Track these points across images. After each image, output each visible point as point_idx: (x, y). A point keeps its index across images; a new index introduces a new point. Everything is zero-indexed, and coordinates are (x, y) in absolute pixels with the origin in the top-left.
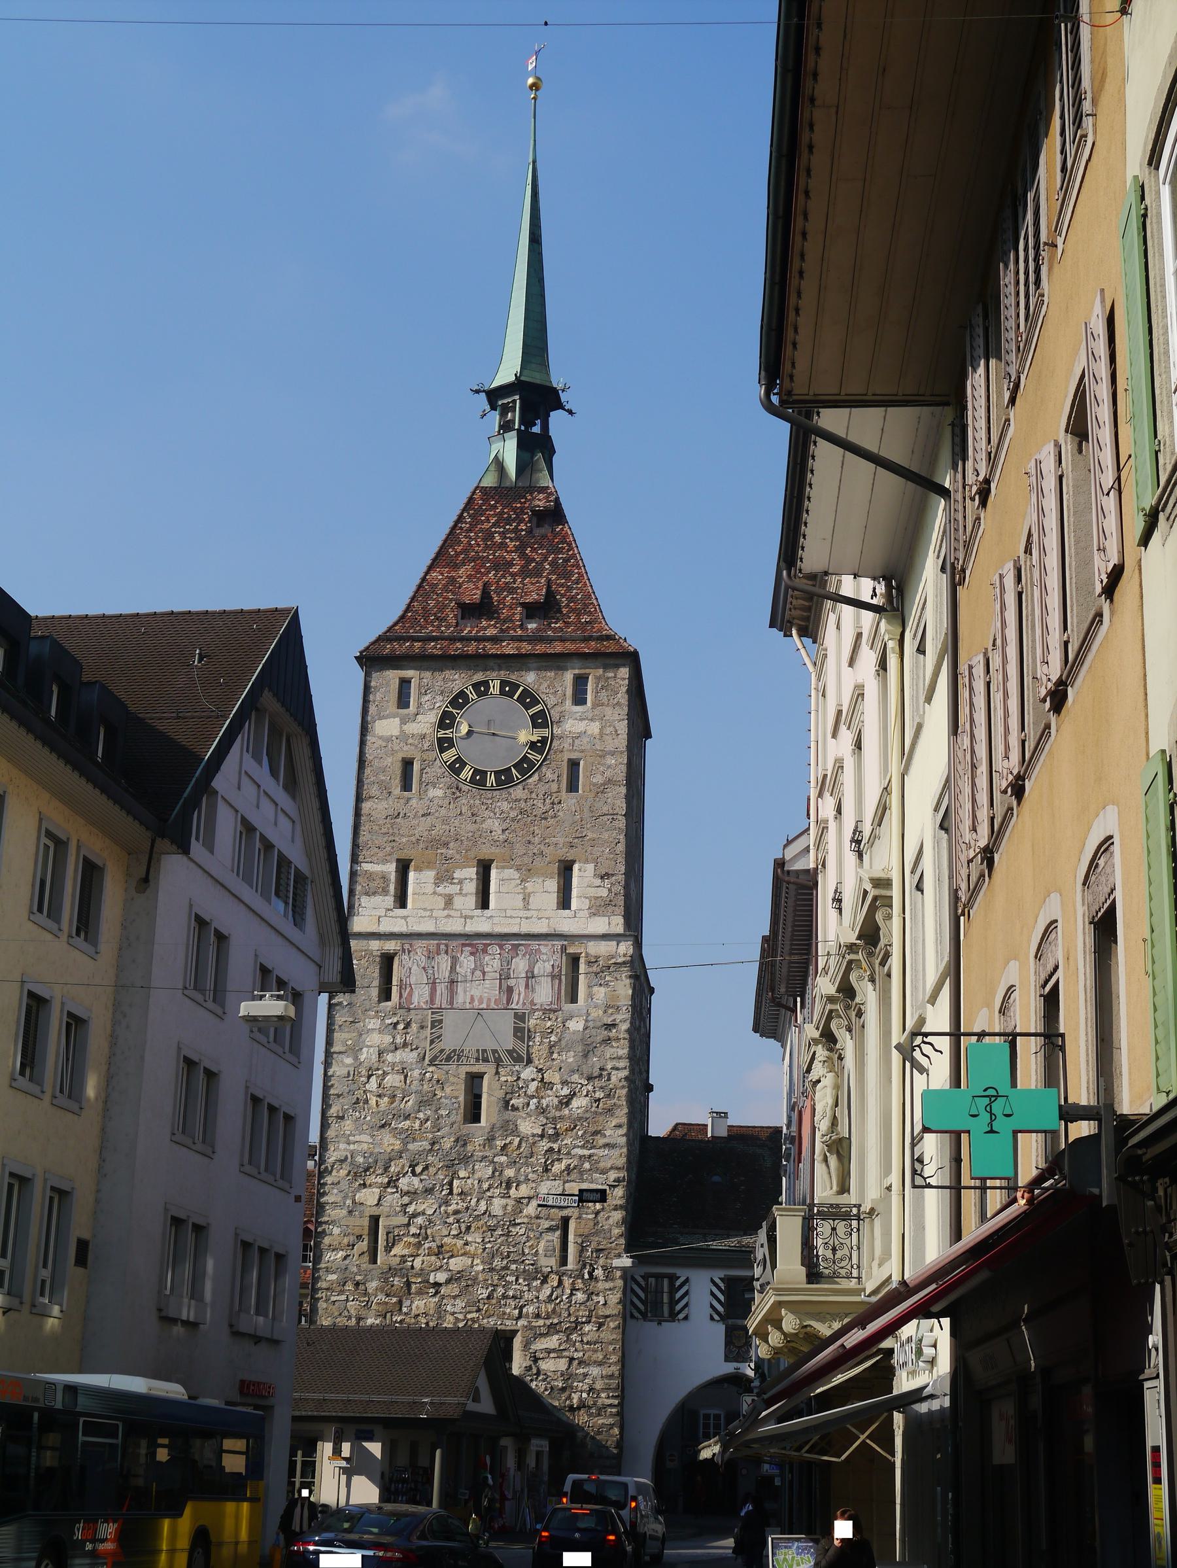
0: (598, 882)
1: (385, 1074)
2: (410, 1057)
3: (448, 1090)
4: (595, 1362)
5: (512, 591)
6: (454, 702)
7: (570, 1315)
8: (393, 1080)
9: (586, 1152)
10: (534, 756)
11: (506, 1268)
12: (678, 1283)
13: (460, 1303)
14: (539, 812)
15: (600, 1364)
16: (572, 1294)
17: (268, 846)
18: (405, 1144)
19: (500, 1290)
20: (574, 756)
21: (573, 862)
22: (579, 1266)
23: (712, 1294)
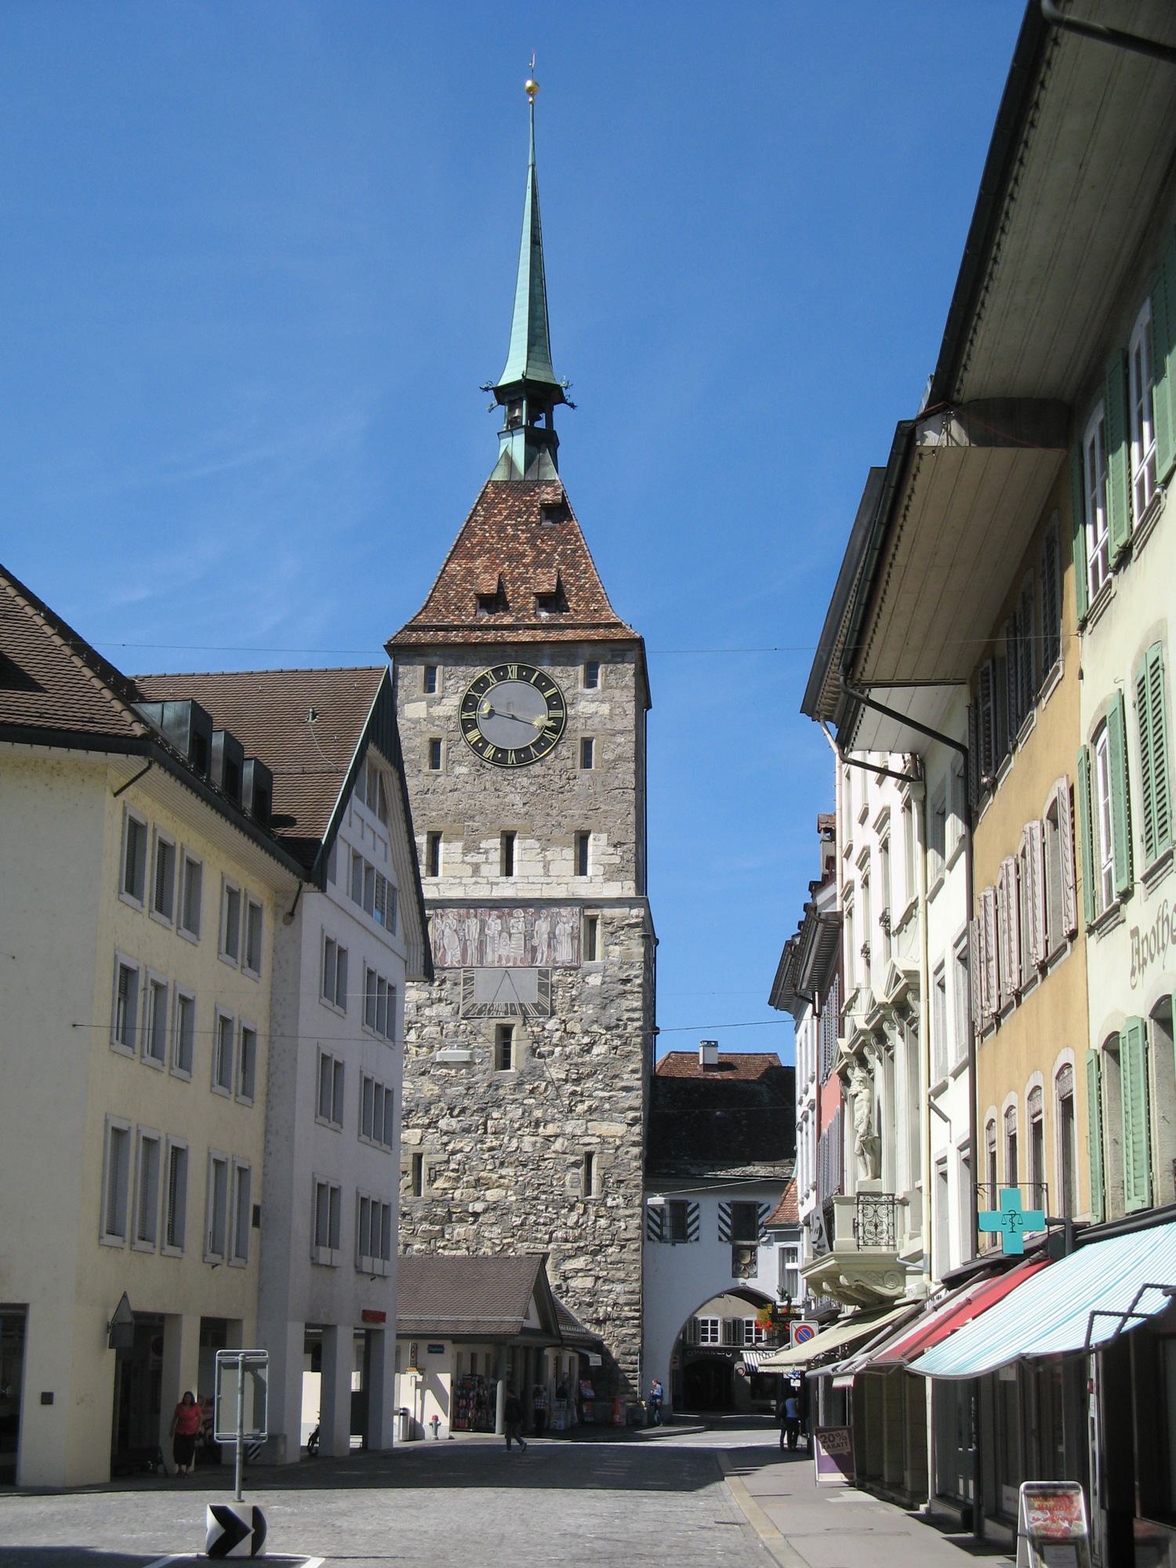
0: (611, 850)
1: (424, 1026)
2: (444, 1010)
3: (480, 1040)
5: (525, 581)
6: (475, 686)
8: (431, 1031)
10: (549, 736)
11: (536, 1198)
12: (689, 1209)
13: (497, 1230)
14: (556, 787)
15: (623, 1281)
17: (369, 869)
18: (443, 1088)
19: (532, 1218)
20: (587, 735)
21: (589, 832)
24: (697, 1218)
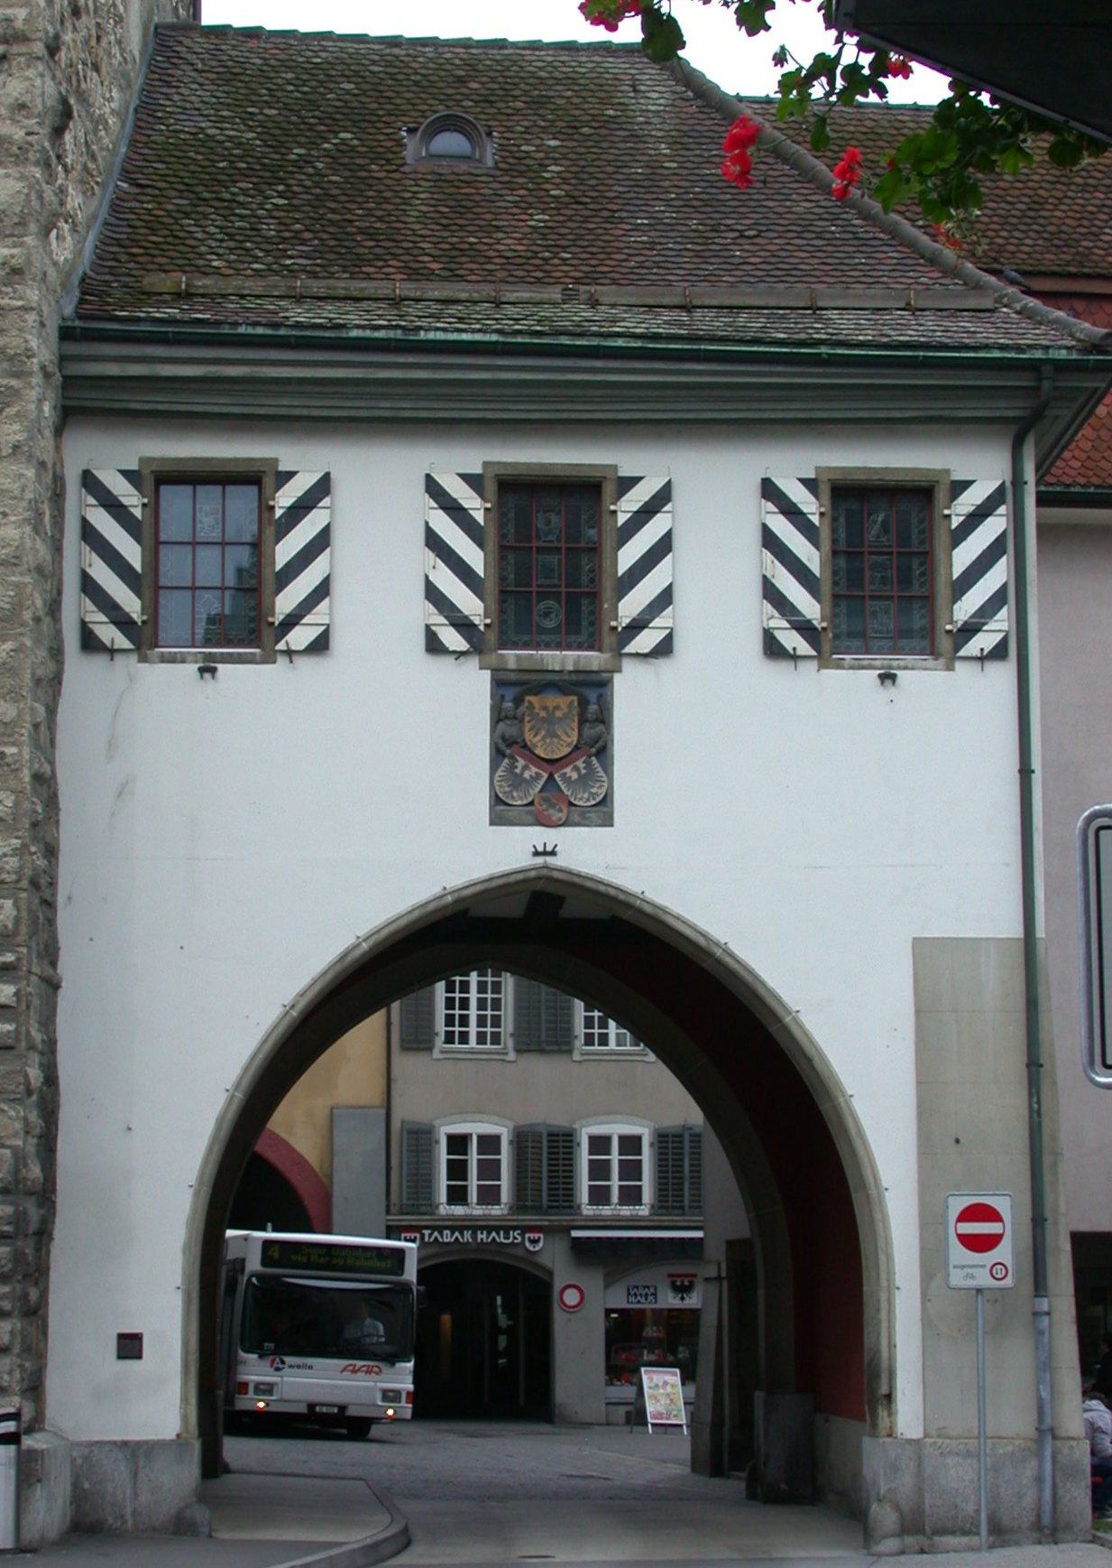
12: (285, 498)
23: (434, 542)
24: (322, 541)
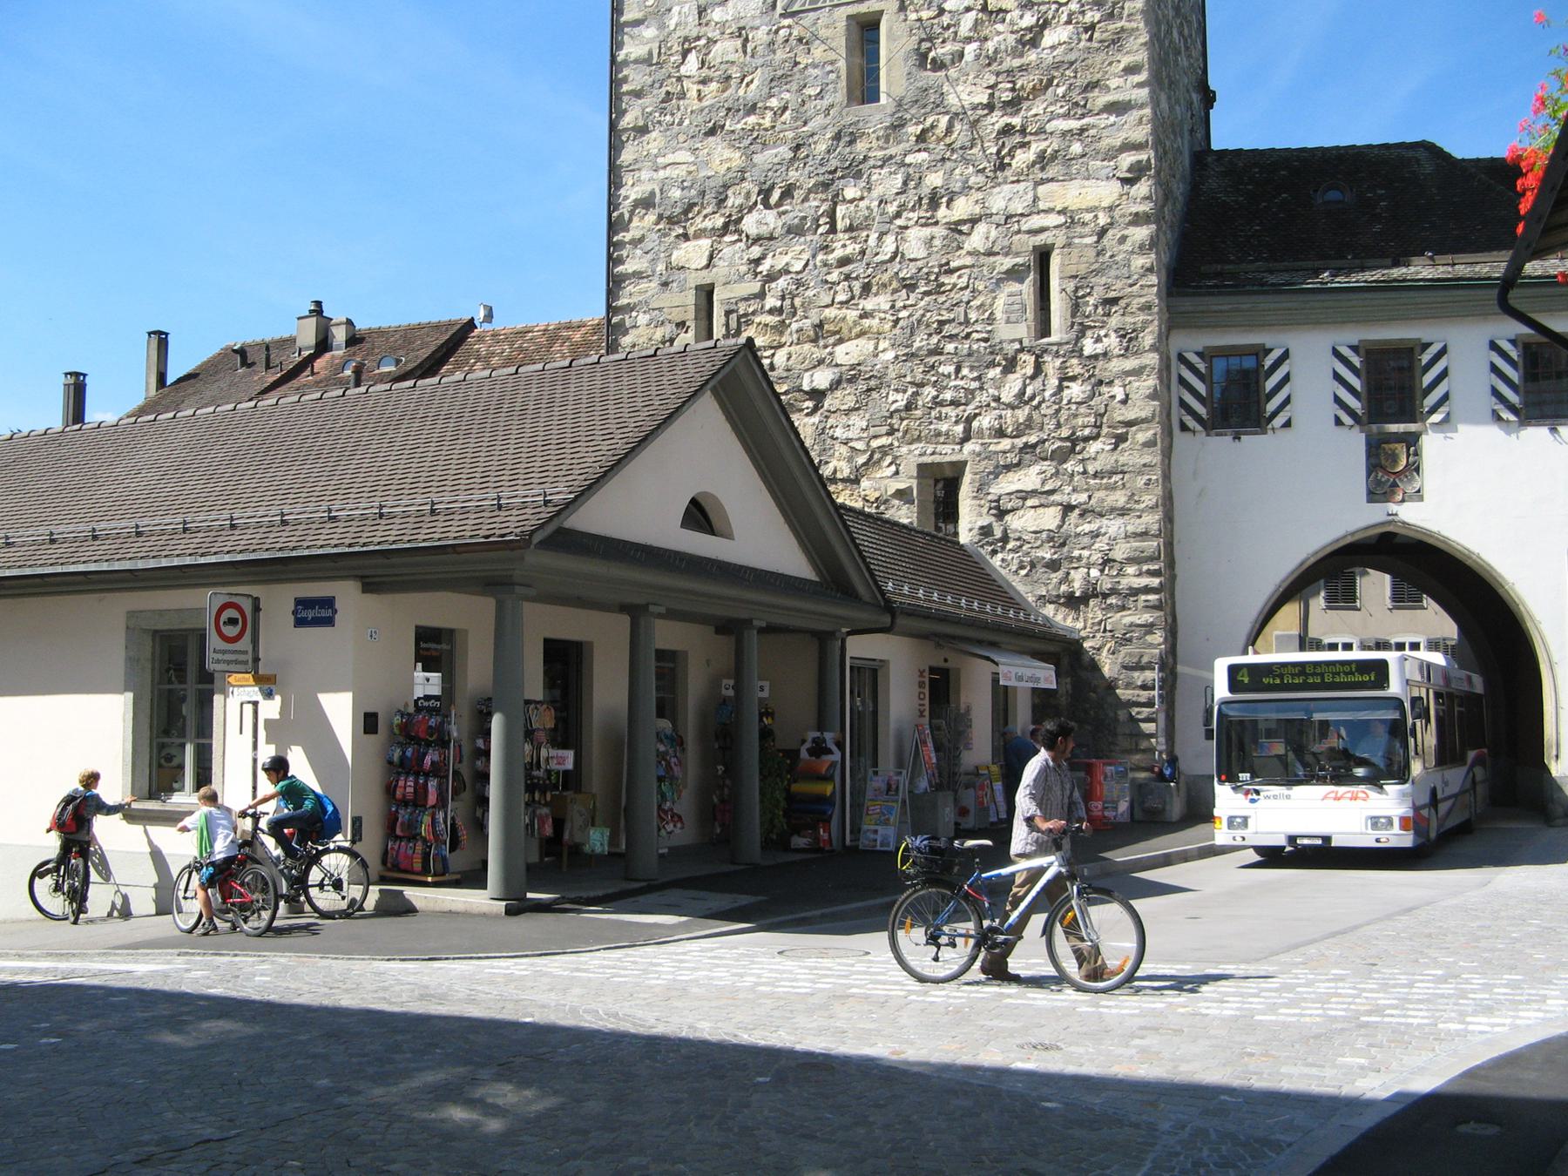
1: (712, 42)
4: (1112, 510)
7: (1059, 426)
9: (1074, 124)
11: (937, 351)
12: (1268, 362)
13: (858, 421)
15: (1123, 512)
16: (1060, 388)
19: (929, 392)
22: (1073, 335)
23: (1337, 377)
24: (1286, 379)
